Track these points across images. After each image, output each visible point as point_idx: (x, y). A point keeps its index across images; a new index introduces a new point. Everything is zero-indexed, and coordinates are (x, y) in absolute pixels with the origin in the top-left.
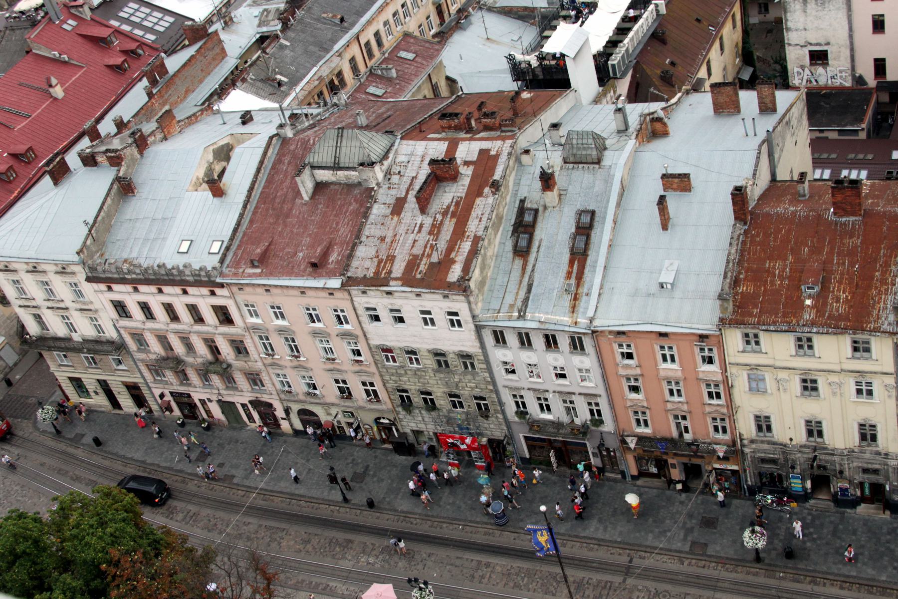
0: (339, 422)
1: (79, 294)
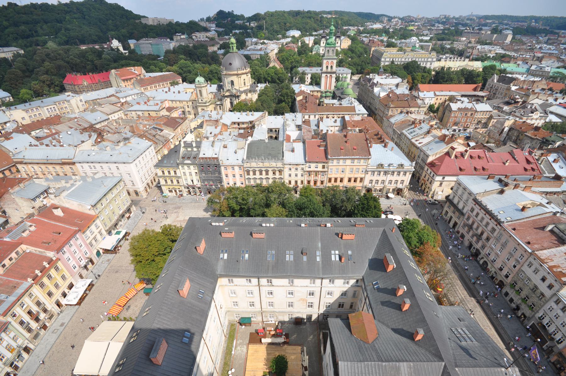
0: (491, 271)
1: (467, 200)
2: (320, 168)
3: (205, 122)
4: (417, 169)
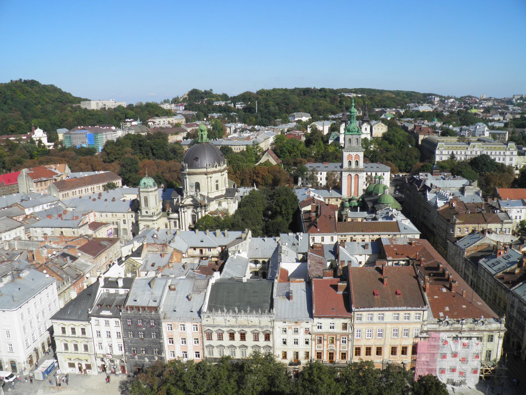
2: (338, 329)
3: (145, 246)
4: (513, 328)
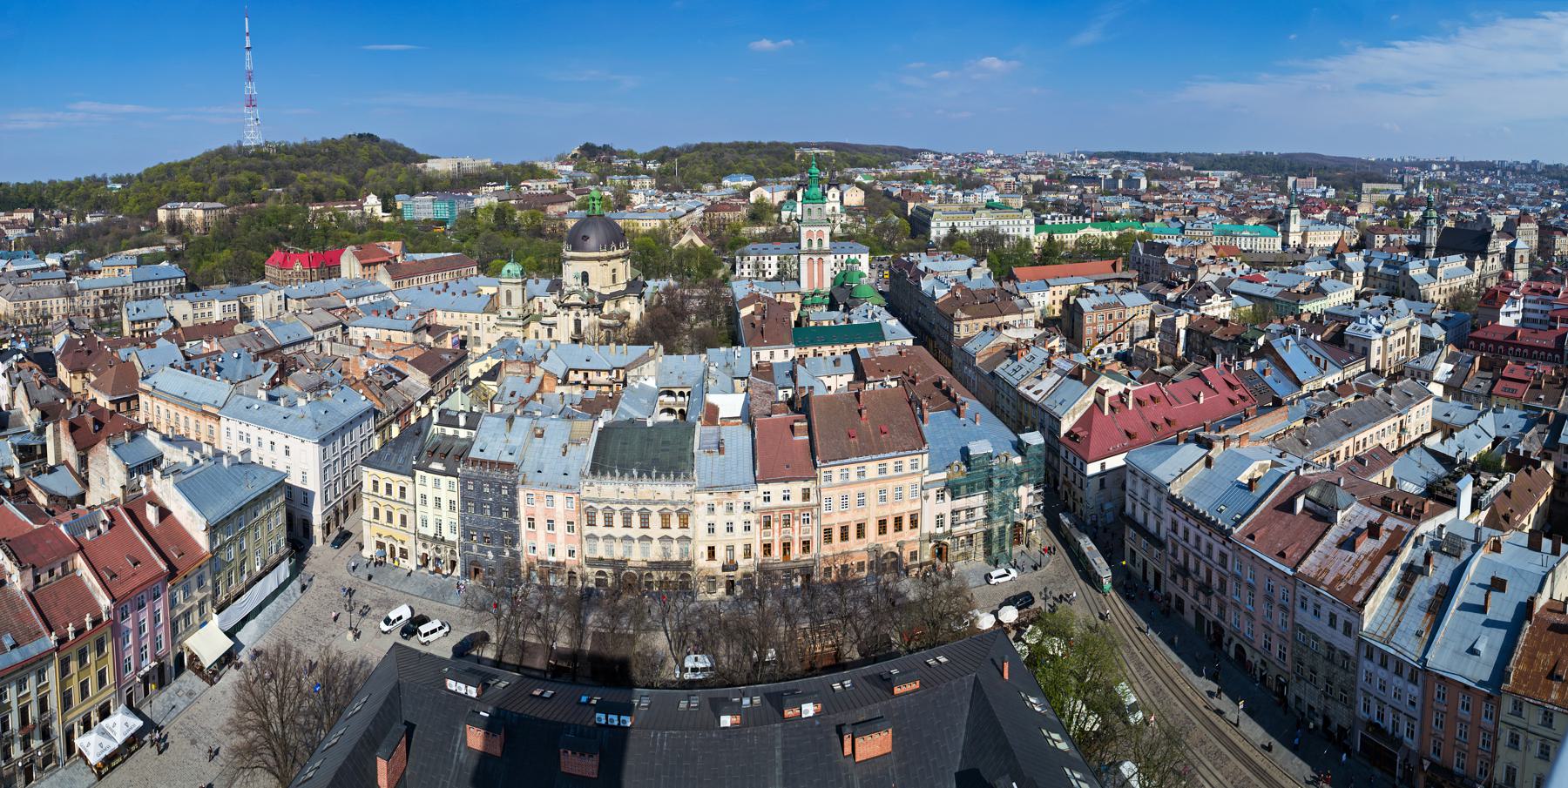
2: (796, 500)
